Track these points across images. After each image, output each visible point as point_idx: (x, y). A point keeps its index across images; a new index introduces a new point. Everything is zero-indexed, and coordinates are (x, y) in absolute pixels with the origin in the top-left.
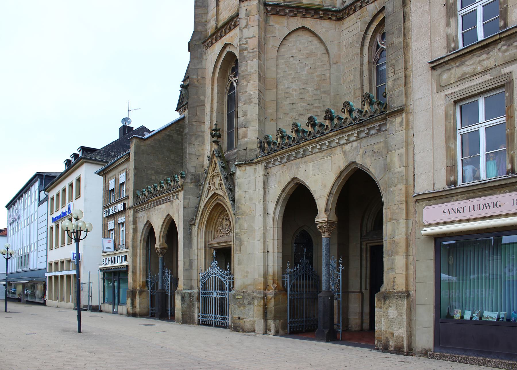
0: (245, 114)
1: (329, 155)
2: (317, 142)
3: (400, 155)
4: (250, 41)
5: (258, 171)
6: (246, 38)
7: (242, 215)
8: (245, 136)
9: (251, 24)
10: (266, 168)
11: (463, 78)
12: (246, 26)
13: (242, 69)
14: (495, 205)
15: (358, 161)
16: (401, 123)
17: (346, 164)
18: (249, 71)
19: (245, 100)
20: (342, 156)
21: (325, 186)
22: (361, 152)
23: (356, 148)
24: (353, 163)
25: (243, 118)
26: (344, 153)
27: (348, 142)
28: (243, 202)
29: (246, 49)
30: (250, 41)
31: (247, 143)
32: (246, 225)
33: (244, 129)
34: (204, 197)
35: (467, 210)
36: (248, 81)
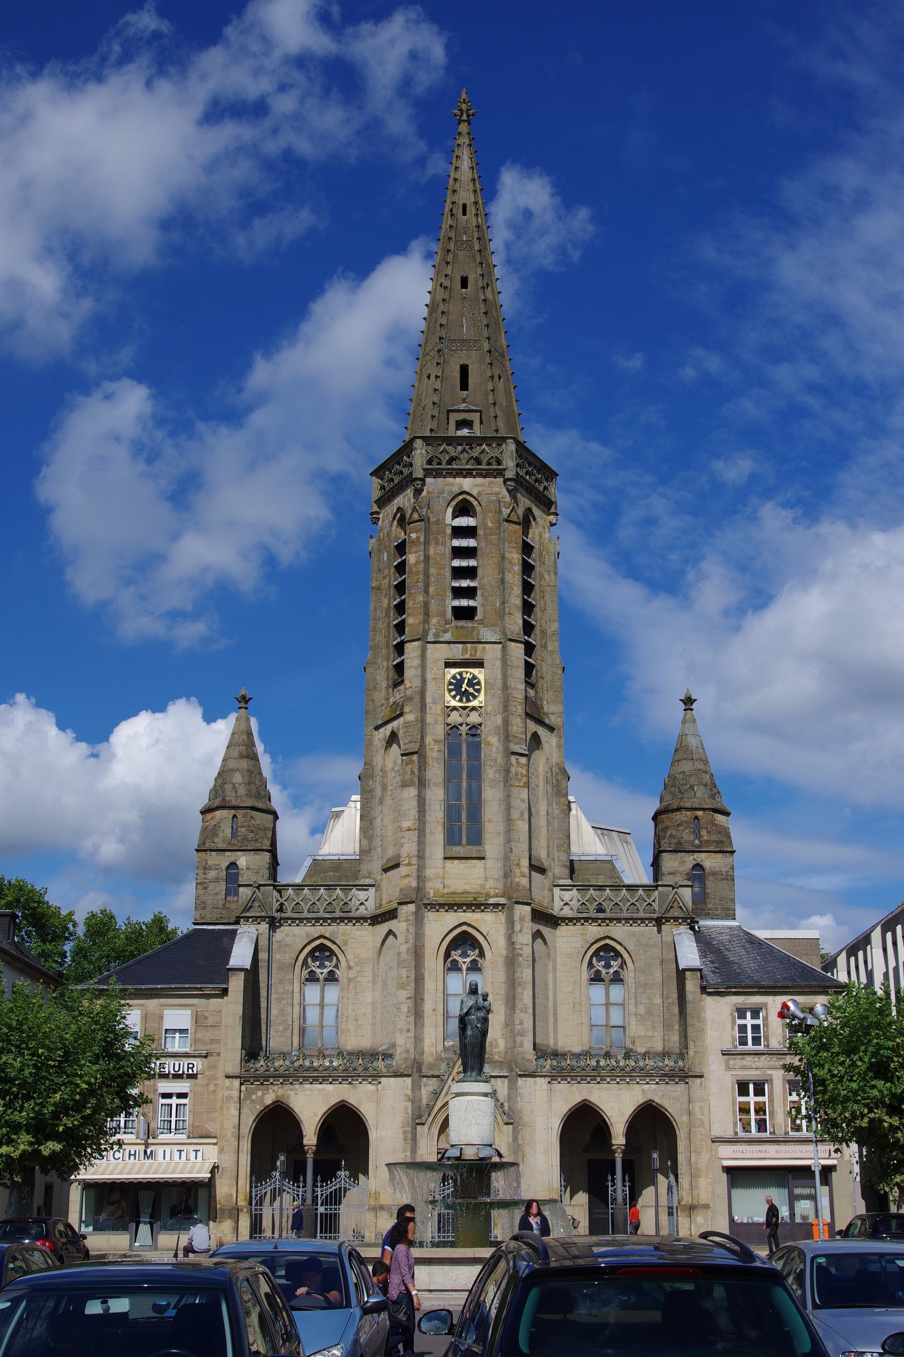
0: (521, 1024)
1: (627, 1089)
2: (618, 1076)
3: (701, 1107)
4: (525, 948)
5: (539, 1084)
6: (520, 944)
7: (524, 1126)
8: (521, 1045)
9: (524, 929)
10: (549, 1082)
11: (743, 1068)
12: (521, 931)
13: (518, 975)
14: (766, 1152)
15: (657, 1100)
16: (701, 1084)
17: (644, 1100)
18: (524, 979)
19: (522, 1009)
20: (640, 1093)
21: (623, 1114)
22: (660, 1094)
23: (654, 1090)
24: (650, 1100)
25: (519, 1026)
26: (643, 1091)
27: (648, 1083)
28: (525, 1113)
29: (521, 955)
30: (525, 948)
31: (523, 1053)
32: (528, 1137)
33: (521, 1038)
34: (441, 1097)
35: (748, 1152)
36: (524, 989)
